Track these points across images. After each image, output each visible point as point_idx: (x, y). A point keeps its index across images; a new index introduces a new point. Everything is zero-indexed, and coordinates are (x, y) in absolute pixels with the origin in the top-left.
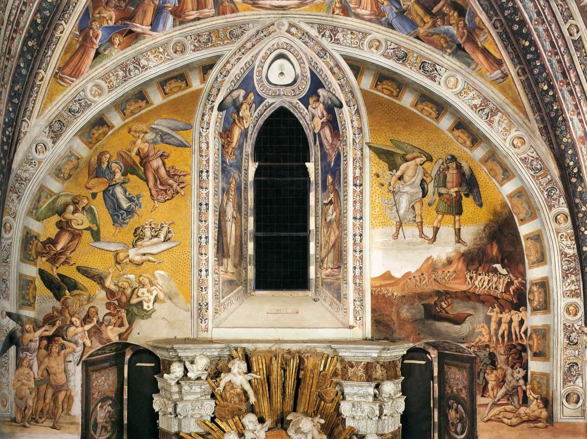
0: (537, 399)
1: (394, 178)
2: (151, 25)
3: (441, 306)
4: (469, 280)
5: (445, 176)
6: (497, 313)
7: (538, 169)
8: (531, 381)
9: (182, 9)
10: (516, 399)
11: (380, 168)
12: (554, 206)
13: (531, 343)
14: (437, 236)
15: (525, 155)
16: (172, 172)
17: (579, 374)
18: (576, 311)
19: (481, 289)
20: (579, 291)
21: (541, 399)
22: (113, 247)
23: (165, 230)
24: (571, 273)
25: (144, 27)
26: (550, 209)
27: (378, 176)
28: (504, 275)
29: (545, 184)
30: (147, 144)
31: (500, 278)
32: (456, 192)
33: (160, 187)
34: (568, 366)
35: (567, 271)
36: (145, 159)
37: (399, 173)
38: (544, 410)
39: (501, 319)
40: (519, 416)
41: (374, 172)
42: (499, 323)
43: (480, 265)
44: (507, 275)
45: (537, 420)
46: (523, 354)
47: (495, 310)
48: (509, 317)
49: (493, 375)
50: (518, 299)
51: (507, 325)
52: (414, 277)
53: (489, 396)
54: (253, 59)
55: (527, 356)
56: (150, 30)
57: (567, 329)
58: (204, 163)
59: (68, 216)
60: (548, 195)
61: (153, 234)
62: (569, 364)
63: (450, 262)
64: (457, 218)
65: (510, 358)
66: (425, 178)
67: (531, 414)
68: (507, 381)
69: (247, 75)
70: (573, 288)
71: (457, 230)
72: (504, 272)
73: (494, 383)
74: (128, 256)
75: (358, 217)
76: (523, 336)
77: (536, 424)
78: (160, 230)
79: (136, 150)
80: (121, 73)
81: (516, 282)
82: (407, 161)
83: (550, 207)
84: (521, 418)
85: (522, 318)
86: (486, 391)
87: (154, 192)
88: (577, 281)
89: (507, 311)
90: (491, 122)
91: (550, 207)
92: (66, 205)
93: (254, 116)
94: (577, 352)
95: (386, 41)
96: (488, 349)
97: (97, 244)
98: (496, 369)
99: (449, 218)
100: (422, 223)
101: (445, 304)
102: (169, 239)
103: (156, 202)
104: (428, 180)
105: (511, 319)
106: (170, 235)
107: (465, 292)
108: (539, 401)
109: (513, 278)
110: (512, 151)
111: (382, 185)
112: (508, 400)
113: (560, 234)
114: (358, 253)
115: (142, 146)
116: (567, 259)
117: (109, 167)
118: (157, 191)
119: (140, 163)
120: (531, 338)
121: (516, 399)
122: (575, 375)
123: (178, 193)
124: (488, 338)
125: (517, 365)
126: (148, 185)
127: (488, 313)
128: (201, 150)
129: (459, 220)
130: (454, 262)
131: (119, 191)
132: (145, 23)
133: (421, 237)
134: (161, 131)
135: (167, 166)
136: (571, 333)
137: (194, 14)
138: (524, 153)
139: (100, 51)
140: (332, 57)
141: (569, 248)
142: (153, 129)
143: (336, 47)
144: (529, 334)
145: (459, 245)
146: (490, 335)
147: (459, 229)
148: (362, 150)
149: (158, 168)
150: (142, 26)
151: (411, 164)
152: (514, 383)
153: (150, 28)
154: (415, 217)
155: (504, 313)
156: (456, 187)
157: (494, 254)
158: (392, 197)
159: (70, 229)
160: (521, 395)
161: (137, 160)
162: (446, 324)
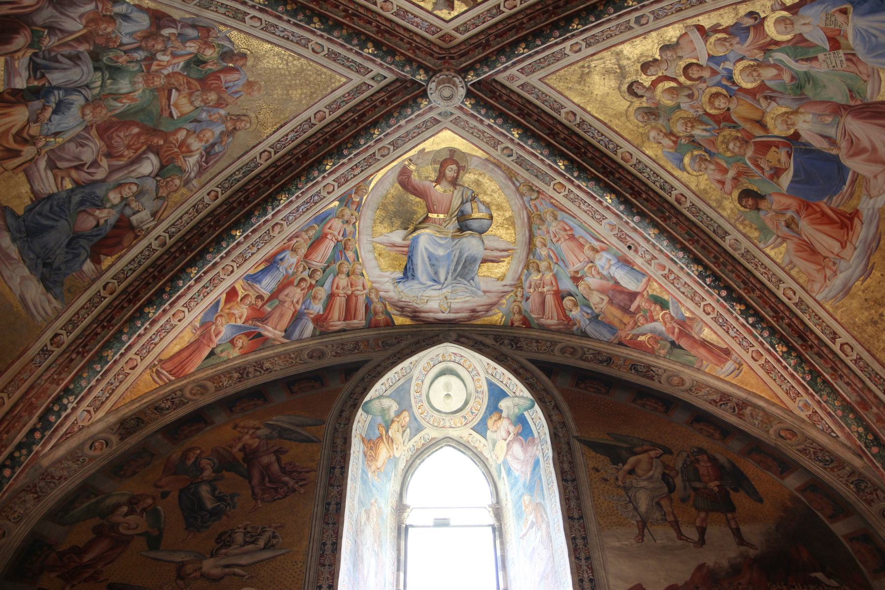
1: (621, 475)
2: (286, 331)
5: (696, 470)
9: (326, 318)
11: (599, 462)
14: (706, 537)
16: (288, 468)
22: (178, 558)
23: (267, 534)
25: (277, 332)
27: (597, 470)
30: (257, 440)
32: (717, 486)
33: (268, 485)
36: (251, 455)
37: (627, 467)
41: (591, 466)
54: (412, 366)
56: (283, 337)
58: (339, 458)
59: (117, 518)
61: (247, 539)
63: (735, 570)
64: (729, 515)
66: (667, 472)
69: (403, 385)
74: (201, 568)
75: (576, 516)
78: (259, 535)
79: (240, 446)
80: (236, 375)
82: (636, 454)
87: (258, 490)
90: (740, 416)
92: (118, 506)
93: (408, 447)
95: (582, 348)
97: (152, 554)
100: (677, 522)
102: (273, 546)
103: (259, 501)
104: (673, 473)
106: (274, 541)
110: (780, 443)
111: (606, 480)
114: (583, 561)
115: (250, 442)
117: (196, 463)
118: (262, 489)
119: (244, 460)
123: (294, 491)
126: (250, 482)
128: (334, 444)
129: (734, 518)
131: (204, 491)
132: (278, 327)
134: (281, 427)
135: (283, 462)
137: (340, 325)
138: (799, 445)
139: (215, 351)
140: (513, 360)
142: (268, 426)
143: (519, 352)
147: (738, 529)
148: (568, 443)
149: (269, 464)
150: (274, 331)
153: (283, 334)
154: (665, 515)
156: (716, 480)
158: (623, 493)
159: (113, 534)
161: (240, 456)
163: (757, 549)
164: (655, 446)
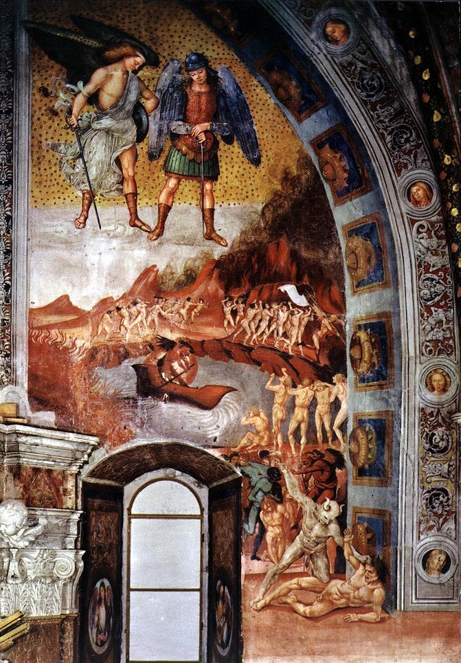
0: (364, 564)
1: (80, 99)
3: (173, 372)
4: (229, 316)
6: (286, 386)
7: (373, 88)
8: (354, 526)
10: (321, 563)
12: (406, 166)
15: (349, 58)
17: (449, 513)
19: (255, 337)
20: (451, 342)
21: (372, 564)
24: (437, 305)
26: (399, 172)
28: (300, 307)
29: (387, 120)
31: (292, 314)
32: (206, 132)
34: (427, 495)
35: (428, 300)
37: (90, 88)
38: (379, 585)
39: (294, 398)
40: (326, 598)
42: (291, 406)
43: (253, 286)
44: (307, 308)
45: (363, 607)
46: (338, 471)
47: (282, 379)
48: (311, 393)
49: (276, 515)
50: (330, 357)
51: (306, 412)
52: (118, 309)
53: (267, 557)
55: (346, 475)
57: (426, 420)
60: (394, 142)
62: (428, 492)
63: (191, 277)
64: (208, 186)
65: (312, 479)
68: (304, 526)
70: (440, 336)
71: (207, 214)
72: (301, 301)
73: (278, 531)
77: (360, 616)
81: (325, 322)
82: (106, 63)
83: (398, 169)
84: (332, 603)
85: (337, 398)
86: (261, 547)
88: (448, 322)
89: (306, 381)
91: (398, 169)
94: (446, 466)
96: (266, 461)
98: (281, 502)
99: (189, 186)
100: (135, 194)
101: (181, 365)
104: (149, 104)
105: (315, 398)
107: (219, 340)
108: (368, 568)
109: (320, 314)
112: (307, 565)
113: (417, 224)
116: (429, 275)
120: (354, 437)
122: (441, 515)
125: (326, 492)
127: (269, 386)
129: (212, 191)
130: (198, 280)
133: (134, 225)
136: (434, 428)
141: (435, 253)
144: (350, 430)
145: (211, 242)
147: (212, 210)
151: (117, 72)
152: (317, 530)
155: (300, 386)
156: (205, 121)
157: (282, 263)
158: (75, 139)
160: (333, 554)
162: (183, 409)
163: (226, 246)
164: (139, 47)
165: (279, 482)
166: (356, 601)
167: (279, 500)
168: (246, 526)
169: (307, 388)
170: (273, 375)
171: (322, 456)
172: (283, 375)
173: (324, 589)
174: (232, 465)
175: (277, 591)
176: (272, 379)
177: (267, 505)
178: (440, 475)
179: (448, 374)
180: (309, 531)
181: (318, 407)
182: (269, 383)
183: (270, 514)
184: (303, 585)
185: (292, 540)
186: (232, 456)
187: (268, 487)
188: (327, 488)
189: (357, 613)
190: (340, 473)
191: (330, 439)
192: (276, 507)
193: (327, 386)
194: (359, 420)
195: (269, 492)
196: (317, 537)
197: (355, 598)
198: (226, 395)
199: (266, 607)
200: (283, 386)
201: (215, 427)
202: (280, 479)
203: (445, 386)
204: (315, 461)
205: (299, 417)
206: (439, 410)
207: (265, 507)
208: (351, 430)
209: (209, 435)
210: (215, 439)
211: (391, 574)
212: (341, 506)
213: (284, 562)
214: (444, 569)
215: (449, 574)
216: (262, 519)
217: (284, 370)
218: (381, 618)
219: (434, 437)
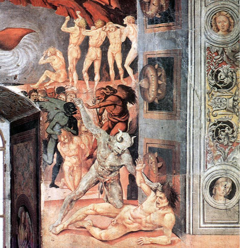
0: (155, 191)
6: (80, 27)
13: (144, 83)
18: (230, 25)
21: (163, 191)
34: (214, 128)
38: (170, 210)
39: (87, 39)
42: (85, 46)
46: (129, 105)
47: (77, 21)
48: (103, 35)
49: (73, 146)
51: (99, 51)
62: (214, 124)
67: (144, 220)
68: (99, 157)
76: (130, 71)
84: (125, 227)
86: (58, 175)
89: (99, 23)
96: (63, 97)
98: (77, 134)
108: (159, 194)
121: (115, 190)
122: (227, 145)
124: (62, 75)
125: (120, 126)
127: (64, 28)
144: (140, 68)
146: (67, 71)
152: (111, 159)
155: (93, 27)
160: (125, 182)
165: (74, 116)
166: (147, 225)
167: (75, 132)
168: (44, 157)
169: (100, 29)
170: (68, 18)
171: (114, 92)
172: (77, 17)
173: (117, 214)
174: (32, 100)
175: (74, 217)
176: (67, 21)
177: (64, 137)
178: (225, 109)
179: (232, 17)
180: (103, 160)
181: (110, 46)
182: (65, 25)
183: (67, 145)
184: (99, 210)
185: (88, 169)
186: (30, 93)
187: (65, 121)
188: (119, 121)
189: (149, 237)
190: (132, 108)
191: (122, 76)
192: (72, 139)
193: (118, 28)
194: (149, 58)
195: (66, 125)
196: (111, 166)
197: (146, 222)
198: (25, 37)
199: (63, 231)
200: (78, 28)
201: (15, 66)
202: (75, 113)
203: (229, 27)
204: (109, 96)
205: (93, 56)
206: (224, 49)
207: (62, 139)
208: (142, 67)
209: (10, 73)
210: (15, 78)
211: (180, 200)
212: (133, 138)
213: (80, 190)
214: (230, 196)
215: (234, 200)
216: (59, 150)
217: (78, 13)
218: (171, 241)
219: (219, 75)
